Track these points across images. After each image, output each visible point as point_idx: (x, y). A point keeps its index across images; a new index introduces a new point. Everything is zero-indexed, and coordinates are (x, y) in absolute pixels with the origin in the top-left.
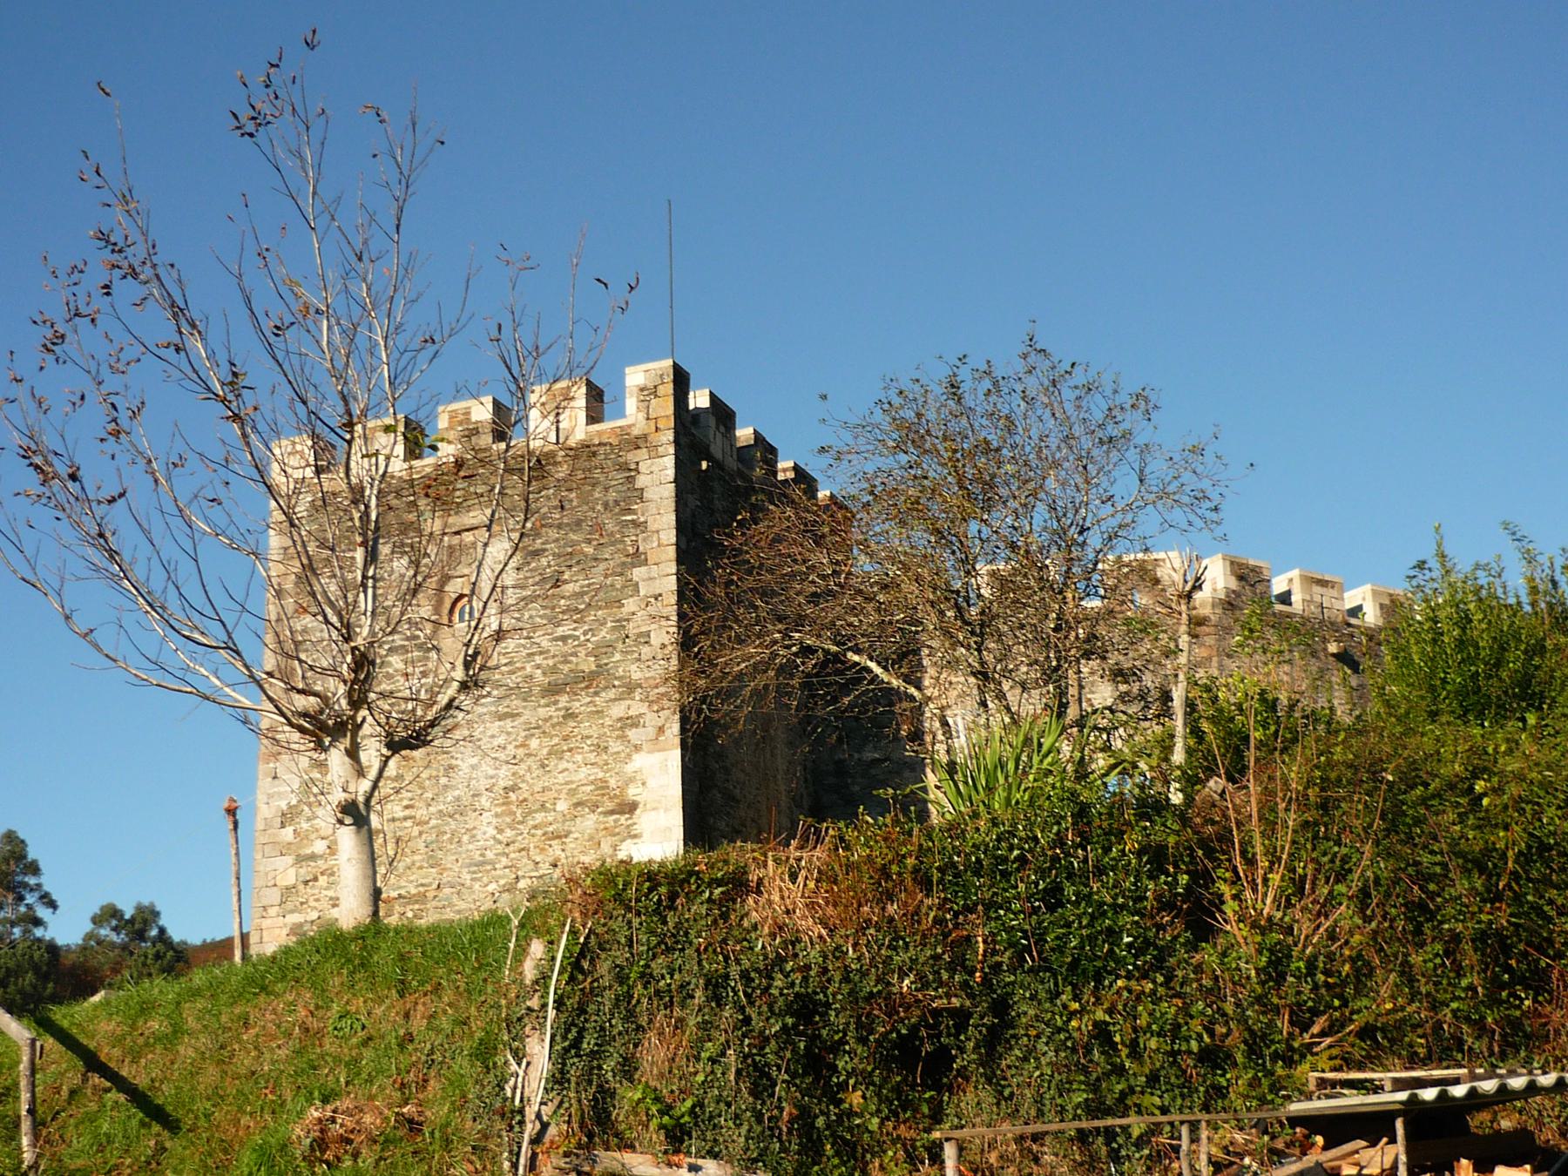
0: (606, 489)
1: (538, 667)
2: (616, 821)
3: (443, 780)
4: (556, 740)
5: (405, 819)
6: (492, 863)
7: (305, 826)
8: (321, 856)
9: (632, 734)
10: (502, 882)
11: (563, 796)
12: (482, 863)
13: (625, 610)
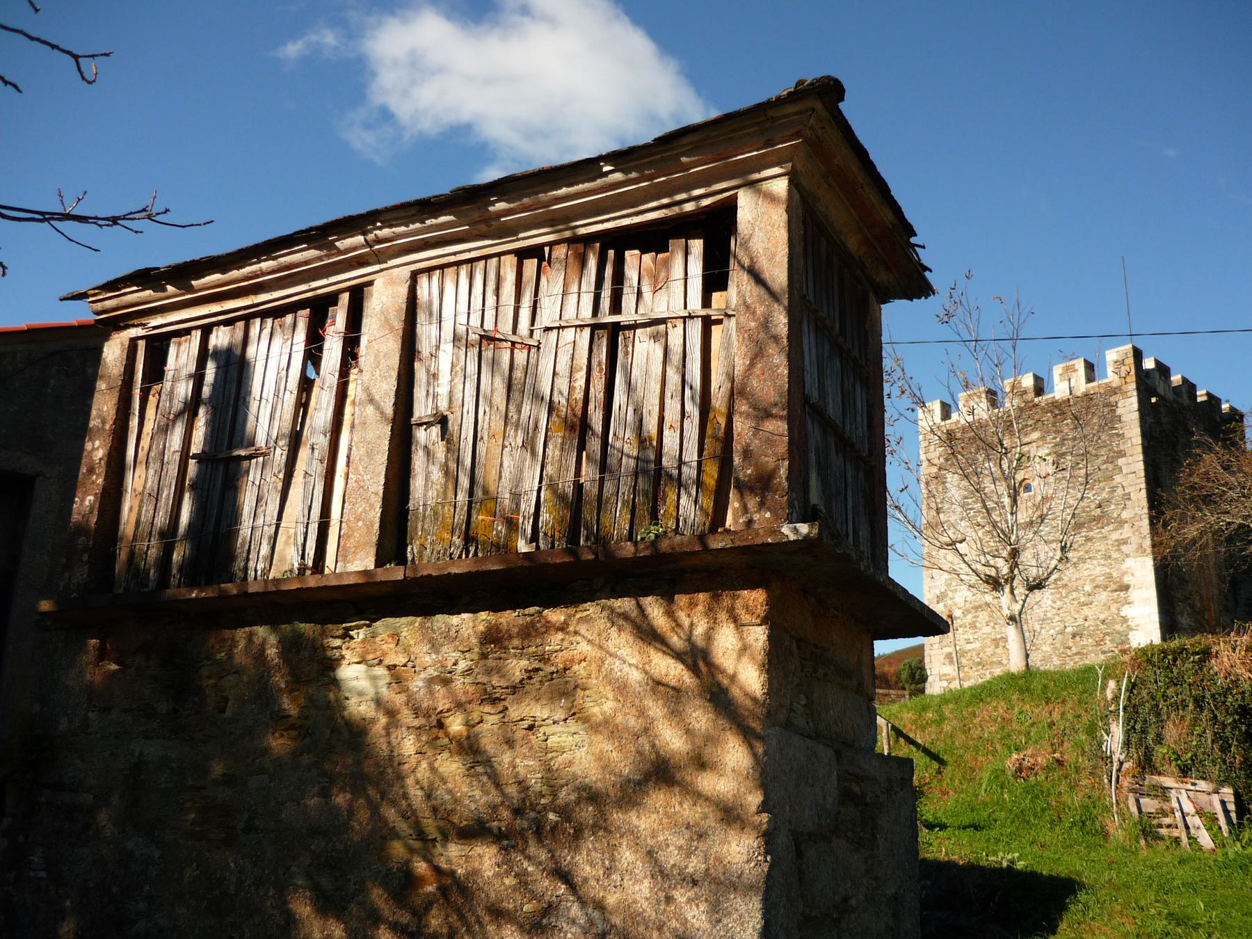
7: (949, 602)
9: (1124, 548)
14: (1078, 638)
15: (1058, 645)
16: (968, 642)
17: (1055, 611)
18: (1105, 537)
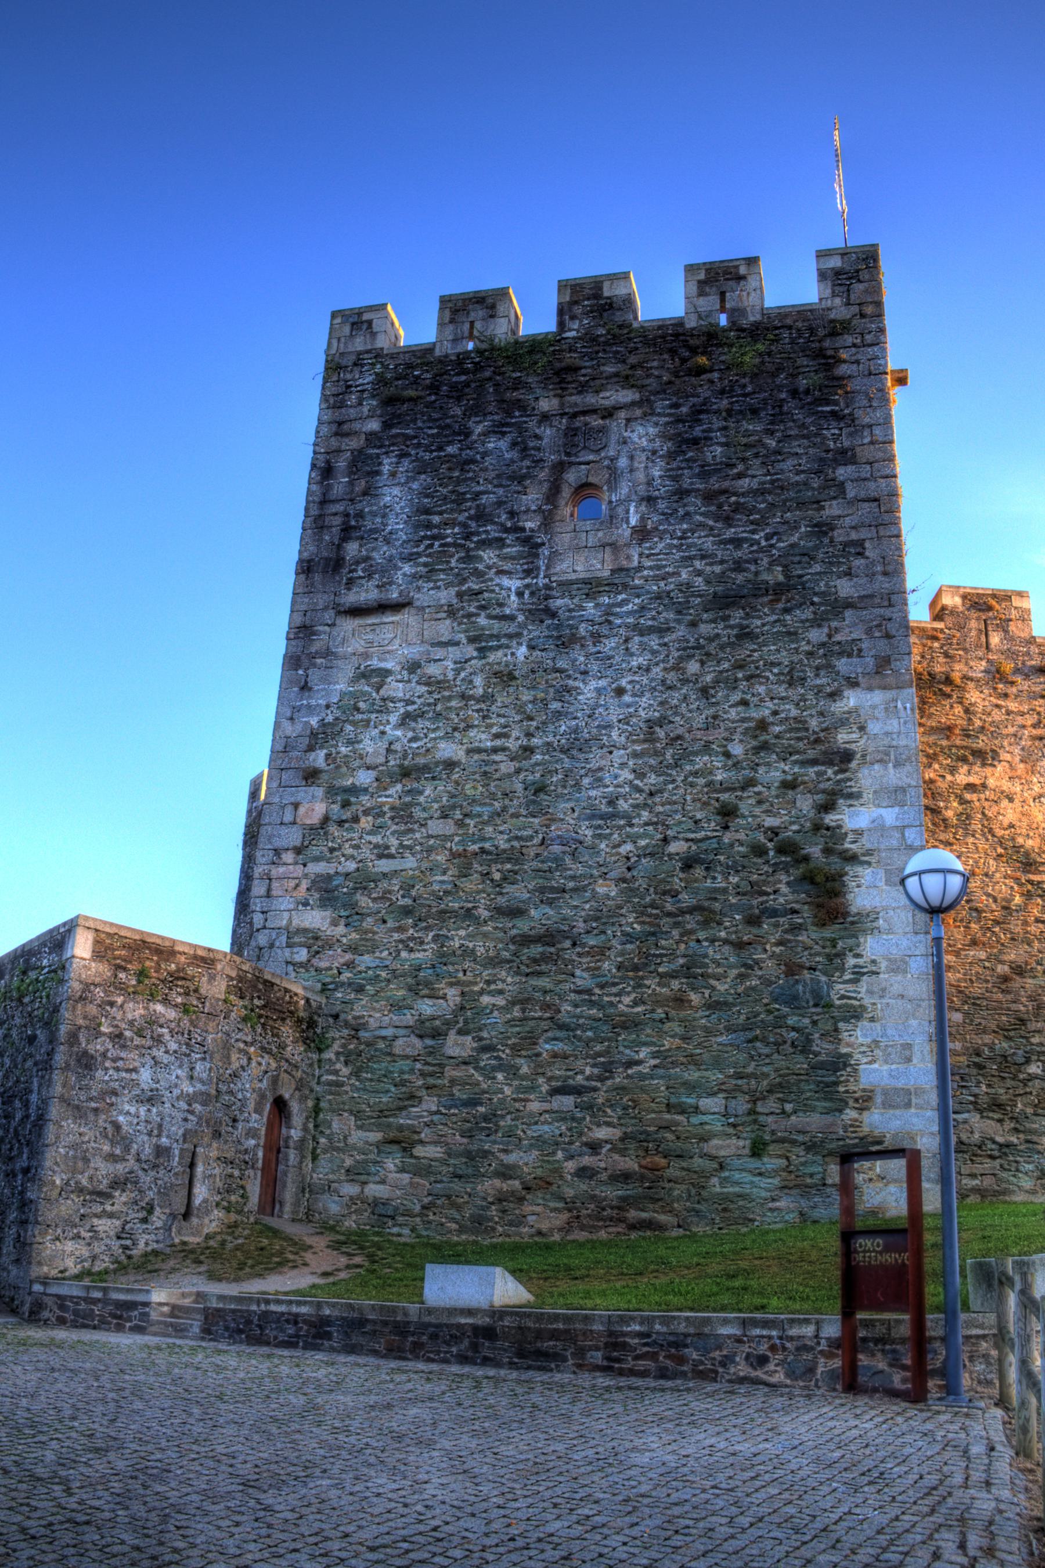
1: (699, 573)
2: (819, 774)
3: (555, 705)
4: (726, 665)
5: (495, 750)
6: (628, 818)
8: (366, 790)
9: (842, 665)
10: (643, 843)
11: (737, 737)
12: (613, 816)
13: (827, 512)
14: (699, 871)
15: (641, 883)
16: (383, 853)
17: (640, 798)
18: (792, 635)
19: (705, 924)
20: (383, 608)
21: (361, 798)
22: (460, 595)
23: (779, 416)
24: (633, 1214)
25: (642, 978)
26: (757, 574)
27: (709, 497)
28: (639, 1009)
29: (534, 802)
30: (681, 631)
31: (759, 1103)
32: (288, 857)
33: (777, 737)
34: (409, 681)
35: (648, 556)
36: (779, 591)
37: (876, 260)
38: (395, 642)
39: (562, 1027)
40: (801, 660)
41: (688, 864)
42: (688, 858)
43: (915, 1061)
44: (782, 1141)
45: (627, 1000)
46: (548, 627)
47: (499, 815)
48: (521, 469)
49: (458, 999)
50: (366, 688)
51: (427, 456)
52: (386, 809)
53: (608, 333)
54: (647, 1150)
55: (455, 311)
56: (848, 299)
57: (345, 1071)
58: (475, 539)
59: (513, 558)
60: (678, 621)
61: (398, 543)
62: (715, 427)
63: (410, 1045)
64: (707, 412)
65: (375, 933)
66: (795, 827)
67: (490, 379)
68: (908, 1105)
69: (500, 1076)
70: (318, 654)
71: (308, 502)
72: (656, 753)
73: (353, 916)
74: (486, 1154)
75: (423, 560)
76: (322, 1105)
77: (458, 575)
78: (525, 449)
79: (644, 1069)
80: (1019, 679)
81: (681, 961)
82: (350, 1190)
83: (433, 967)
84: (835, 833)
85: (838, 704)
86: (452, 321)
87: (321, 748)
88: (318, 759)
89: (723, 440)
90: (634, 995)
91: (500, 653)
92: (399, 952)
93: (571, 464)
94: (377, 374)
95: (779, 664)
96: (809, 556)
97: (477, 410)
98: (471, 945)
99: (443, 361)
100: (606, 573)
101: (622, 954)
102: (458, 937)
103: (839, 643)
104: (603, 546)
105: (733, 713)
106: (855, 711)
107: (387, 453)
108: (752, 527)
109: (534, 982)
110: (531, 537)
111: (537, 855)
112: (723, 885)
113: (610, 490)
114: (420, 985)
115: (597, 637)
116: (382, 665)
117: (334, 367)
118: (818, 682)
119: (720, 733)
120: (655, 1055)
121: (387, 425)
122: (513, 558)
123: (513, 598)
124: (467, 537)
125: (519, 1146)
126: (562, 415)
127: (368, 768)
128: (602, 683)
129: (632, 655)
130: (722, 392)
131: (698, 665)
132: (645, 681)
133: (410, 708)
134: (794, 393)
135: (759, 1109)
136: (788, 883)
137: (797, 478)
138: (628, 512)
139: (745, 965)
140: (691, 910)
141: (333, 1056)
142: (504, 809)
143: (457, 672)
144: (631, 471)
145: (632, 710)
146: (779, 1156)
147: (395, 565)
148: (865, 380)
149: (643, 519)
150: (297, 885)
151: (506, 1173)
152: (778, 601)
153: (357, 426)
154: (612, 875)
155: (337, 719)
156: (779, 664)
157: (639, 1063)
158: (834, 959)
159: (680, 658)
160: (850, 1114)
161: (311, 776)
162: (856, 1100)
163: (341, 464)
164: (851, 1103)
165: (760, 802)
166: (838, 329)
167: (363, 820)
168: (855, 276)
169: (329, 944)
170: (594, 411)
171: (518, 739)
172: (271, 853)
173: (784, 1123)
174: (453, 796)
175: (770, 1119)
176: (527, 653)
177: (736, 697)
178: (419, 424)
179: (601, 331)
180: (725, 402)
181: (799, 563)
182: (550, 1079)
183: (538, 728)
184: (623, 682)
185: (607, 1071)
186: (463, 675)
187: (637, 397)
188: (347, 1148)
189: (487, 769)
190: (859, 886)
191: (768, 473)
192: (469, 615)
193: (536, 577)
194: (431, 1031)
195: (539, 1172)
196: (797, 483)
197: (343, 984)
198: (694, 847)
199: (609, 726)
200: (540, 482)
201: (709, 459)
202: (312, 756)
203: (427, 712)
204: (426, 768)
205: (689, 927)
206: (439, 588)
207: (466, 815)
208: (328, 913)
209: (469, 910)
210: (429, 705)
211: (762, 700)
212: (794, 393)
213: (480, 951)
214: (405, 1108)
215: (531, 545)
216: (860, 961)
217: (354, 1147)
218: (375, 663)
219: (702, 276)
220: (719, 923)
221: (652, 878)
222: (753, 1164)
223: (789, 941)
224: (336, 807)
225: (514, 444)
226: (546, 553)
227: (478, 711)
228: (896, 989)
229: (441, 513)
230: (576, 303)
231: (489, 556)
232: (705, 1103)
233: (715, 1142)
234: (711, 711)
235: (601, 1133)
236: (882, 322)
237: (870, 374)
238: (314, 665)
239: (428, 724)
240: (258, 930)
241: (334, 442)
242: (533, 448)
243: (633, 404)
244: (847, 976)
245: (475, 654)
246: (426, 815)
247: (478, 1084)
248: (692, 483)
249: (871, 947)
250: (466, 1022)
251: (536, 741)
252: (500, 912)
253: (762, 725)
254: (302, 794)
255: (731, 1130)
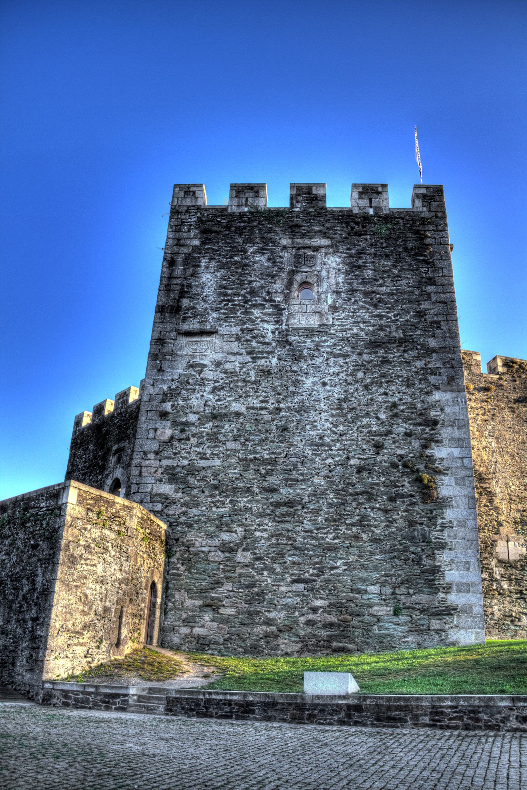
0: (405, 241)
1: (362, 330)
2: (422, 430)
3: (292, 389)
4: (376, 375)
5: (261, 409)
7: (181, 403)
8: (193, 424)
9: (432, 379)
10: (337, 459)
11: (382, 410)
12: (323, 445)
14: (365, 474)
15: (337, 479)
16: (203, 457)
17: (336, 437)
18: (408, 363)
19: (369, 500)
20: (202, 333)
21: (191, 428)
22: (242, 330)
23: (399, 259)
24: (335, 644)
25: (338, 526)
26: (390, 332)
27: (366, 294)
28: (337, 541)
29: (282, 436)
30: (354, 357)
31: (397, 589)
32: (152, 456)
33: (402, 411)
34: (216, 371)
35: (337, 320)
36: (401, 341)
37: (442, 192)
38: (209, 351)
39: (297, 549)
40: (412, 376)
41: (360, 470)
42: (360, 468)
43: (471, 570)
44: (409, 608)
45: (330, 536)
46: (288, 350)
47: (264, 441)
48: (273, 271)
49: (243, 533)
50: (193, 373)
51: (224, 261)
52: (204, 434)
53: (315, 211)
54: (341, 612)
55: (238, 192)
56: (430, 208)
57: (183, 568)
58: (250, 303)
59: (269, 314)
60: (353, 352)
61: (210, 302)
62: (369, 261)
63: (216, 556)
64: (365, 253)
65: (198, 497)
66: (411, 455)
67: (256, 226)
68: (468, 591)
69: (265, 573)
70: (167, 354)
71: (161, 277)
72: (343, 415)
73: (186, 488)
74: (258, 613)
75: (223, 311)
76: (170, 585)
77: (241, 320)
78: (275, 262)
79: (339, 571)
80: (476, 392)
81: (357, 518)
82: (185, 630)
83: (230, 516)
84: (431, 459)
85: (431, 397)
86: (237, 196)
87: (169, 401)
88: (168, 406)
89: (373, 268)
90: (334, 534)
91: (263, 361)
92: (211, 507)
93: (298, 272)
94: (198, 218)
95: (402, 376)
96: (415, 326)
97: (250, 241)
98: (250, 506)
99: (232, 215)
100: (317, 326)
101: (327, 513)
102: (243, 502)
103: (430, 368)
104: (315, 313)
105: (380, 398)
106: (439, 401)
107: (203, 257)
108: (387, 310)
109: (283, 526)
110: (278, 305)
111: (284, 462)
112: (377, 481)
113: (318, 286)
114: (222, 525)
115: (312, 357)
116: (202, 362)
117: (175, 212)
118: (421, 386)
119: (374, 408)
120: (345, 564)
121: (203, 243)
122: (269, 314)
123: (270, 334)
124: (246, 302)
125: (275, 609)
126: (293, 247)
127: (194, 413)
128: (316, 379)
129: (330, 367)
130: (372, 245)
131: (362, 374)
132: (337, 380)
133: (216, 384)
134: (406, 249)
135: (397, 592)
136: (409, 482)
137: (408, 289)
138: (327, 297)
139: (388, 521)
140: (362, 493)
141: (176, 560)
142: (266, 438)
143: (241, 368)
144: (328, 278)
145: (330, 393)
146: (407, 616)
147: (208, 313)
148: (439, 247)
149: (334, 301)
150: (156, 471)
151: (269, 622)
152: (401, 346)
153: (188, 242)
154: (322, 474)
155: (177, 387)
156: (402, 376)
157: (337, 568)
158: (432, 520)
159: (354, 370)
160: (441, 595)
161: (164, 415)
162: (444, 588)
163: (180, 259)
164: (441, 590)
165: (394, 442)
166: (424, 221)
167: (192, 439)
168: (433, 198)
169: (173, 502)
170: (309, 248)
171: (273, 404)
172: (142, 454)
173: (410, 599)
174: (240, 430)
175: (402, 597)
176: (277, 362)
177: (382, 391)
178: (220, 244)
179: (312, 210)
180: (373, 250)
181: (410, 329)
182: (292, 575)
183: (283, 399)
184: (326, 380)
185: (321, 571)
186: (244, 370)
187: (330, 243)
188: (183, 608)
189: (257, 417)
190: (442, 485)
191: (394, 286)
192: (247, 341)
193: (281, 325)
194: (229, 549)
195: (286, 622)
196: (408, 292)
197: (181, 523)
198: (362, 462)
199: (319, 401)
200: (283, 279)
201: (366, 276)
202: (164, 405)
203: (226, 387)
204: (225, 415)
205: (361, 501)
206: (231, 326)
207: (246, 440)
208: (173, 486)
209: (248, 488)
210: (227, 383)
211: (394, 393)
212: (406, 249)
213: (255, 509)
214: (215, 588)
215: (279, 310)
216: (444, 521)
217: (187, 608)
218: (198, 360)
219: (360, 190)
220: (376, 500)
221: (342, 477)
222: (395, 619)
223: (410, 510)
224: (177, 432)
225: (269, 259)
226: (286, 313)
227: (252, 388)
228: (461, 535)
229: (232, 289)
230: (299, 195)
231: (257, 312)
232: (371, 588)
233: (376, 608)
234: (369, 397)
235: (318, 603)
236: (445, 221)
237: (441, 244)
238: (165, 359)
239: (226, 393)
240: (134, 493)
241: (176, 249)
242: (279, 262)
243: (328, 246)
244: (438, 528)
245: (250, 360)
246: (225, 439)
247: (254, 577)
248: (358, 287)
249: (450, 514)
250: (247, 545)
251: (282, 405)
252: (265, 490)
253: (395, 405)
254: (159, 424)
255: (383, 602)
